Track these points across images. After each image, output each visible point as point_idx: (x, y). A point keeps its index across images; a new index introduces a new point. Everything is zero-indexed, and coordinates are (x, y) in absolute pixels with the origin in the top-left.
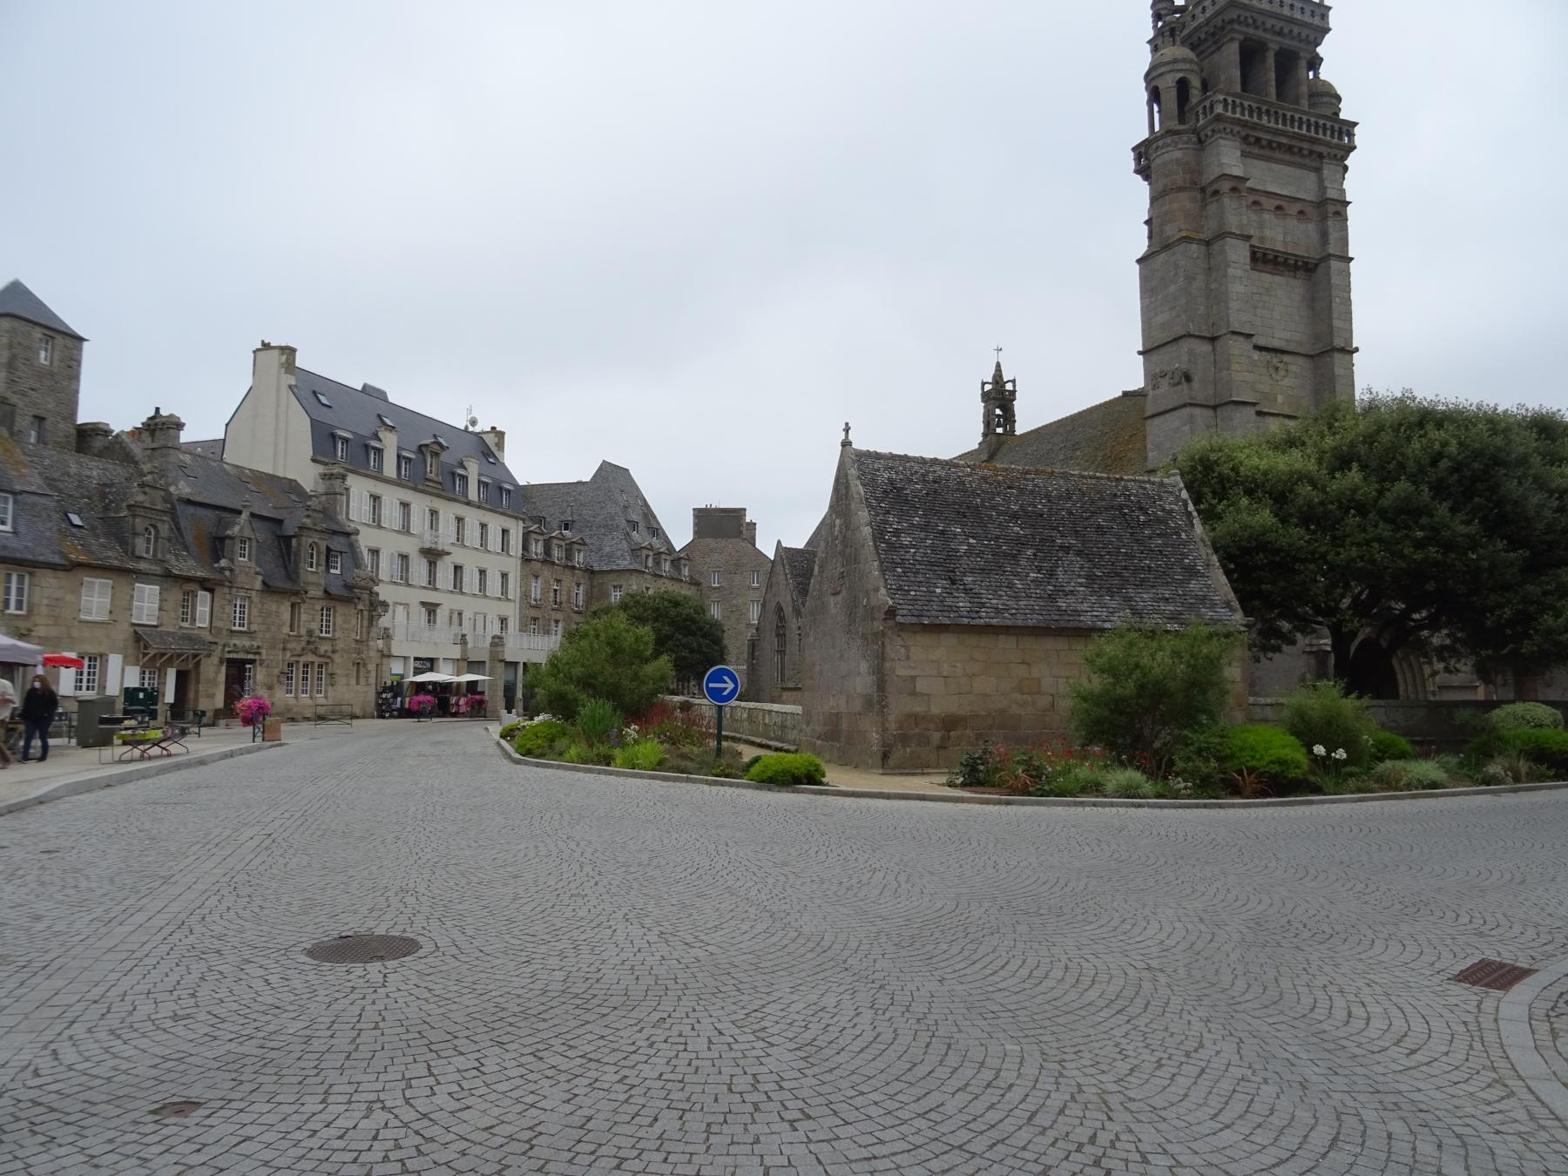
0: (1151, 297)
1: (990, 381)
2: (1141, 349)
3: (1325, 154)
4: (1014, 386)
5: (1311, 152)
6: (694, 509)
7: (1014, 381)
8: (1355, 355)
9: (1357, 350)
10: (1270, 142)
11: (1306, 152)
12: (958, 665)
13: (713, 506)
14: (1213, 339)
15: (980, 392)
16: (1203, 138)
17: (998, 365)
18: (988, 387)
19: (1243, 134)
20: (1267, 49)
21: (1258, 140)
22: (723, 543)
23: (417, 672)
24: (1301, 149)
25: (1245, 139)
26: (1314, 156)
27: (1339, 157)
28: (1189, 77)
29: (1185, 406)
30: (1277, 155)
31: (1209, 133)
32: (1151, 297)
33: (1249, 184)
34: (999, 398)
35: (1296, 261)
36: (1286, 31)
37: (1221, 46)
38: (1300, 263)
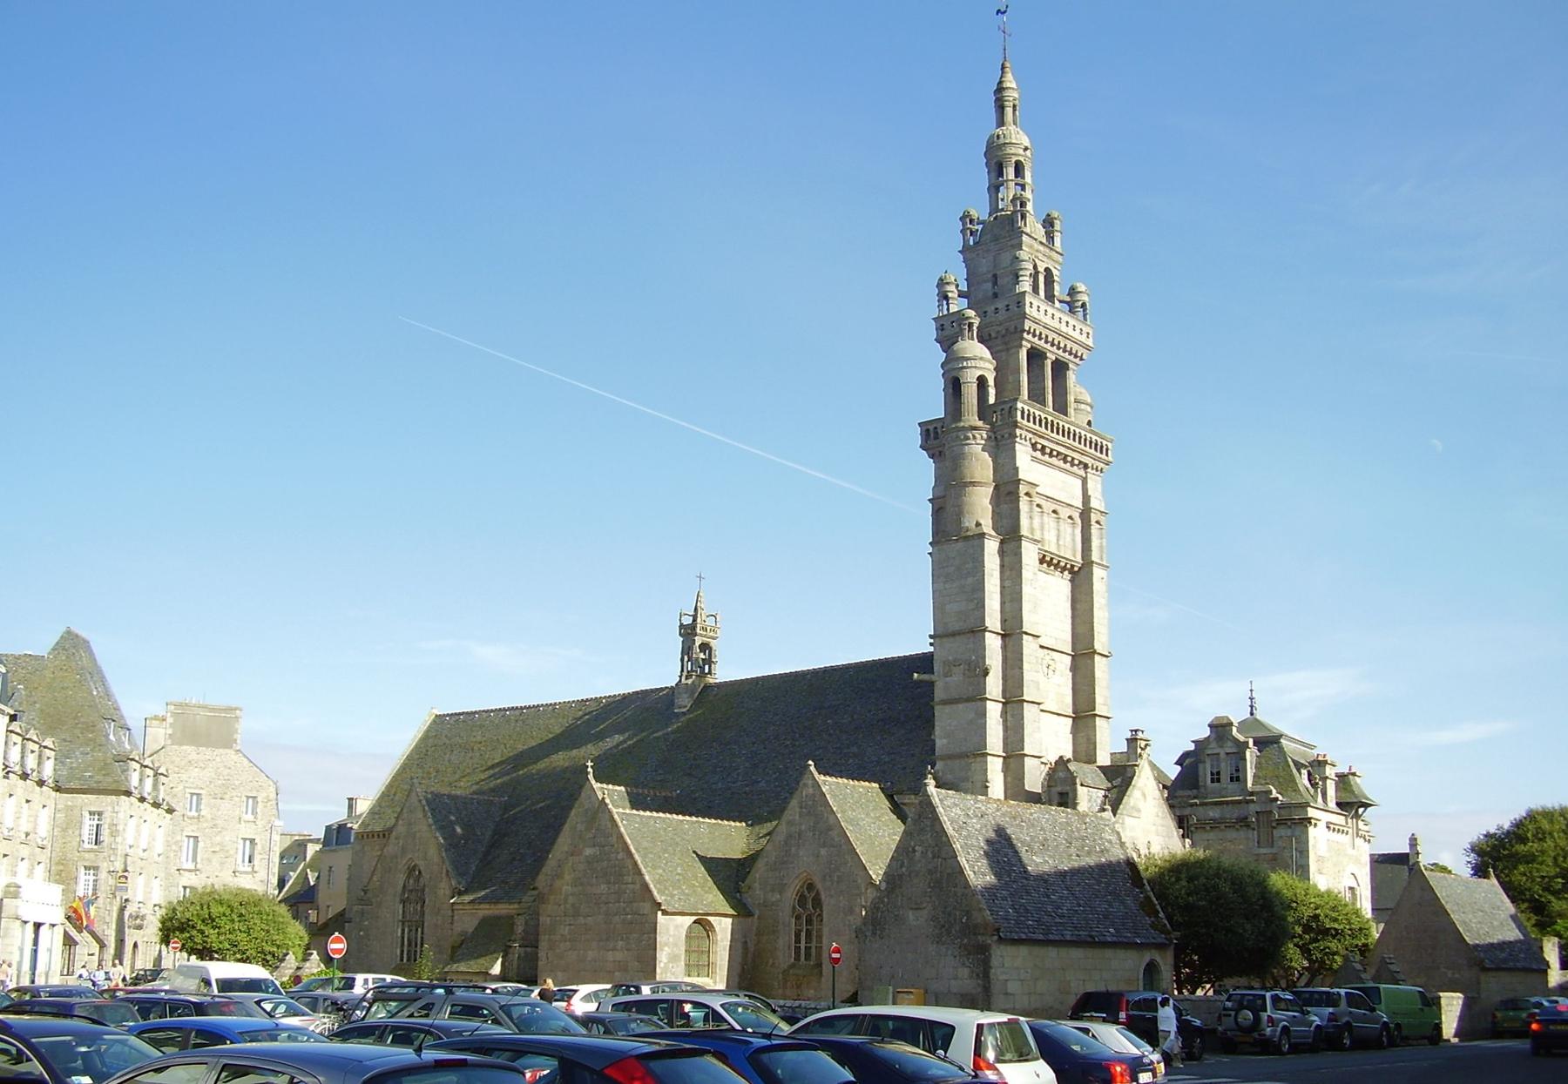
0: (944, 583)
2: (932, 633)
3: (1090, 465)
5: (1080, 462)
10: (1052, 450)
11: (1076, 462)
12: (1029, 971)
16: (999, 437)
19: (1033, 441)
20: (1046, 358)
21: (1044, 447)
22: (207, 753)
23: (1234, 990)
24: (1073, 459)
25: (1034, 446)
26: (1081, 466)
28: (986, 375)
30: (1054, 460)
31: (1006, 436)
32: (944, 583)
33: (1038, 490)
34: (1155, 799)
35: (1066, 564)
37: (1012, 348)
38: (1068, 566)
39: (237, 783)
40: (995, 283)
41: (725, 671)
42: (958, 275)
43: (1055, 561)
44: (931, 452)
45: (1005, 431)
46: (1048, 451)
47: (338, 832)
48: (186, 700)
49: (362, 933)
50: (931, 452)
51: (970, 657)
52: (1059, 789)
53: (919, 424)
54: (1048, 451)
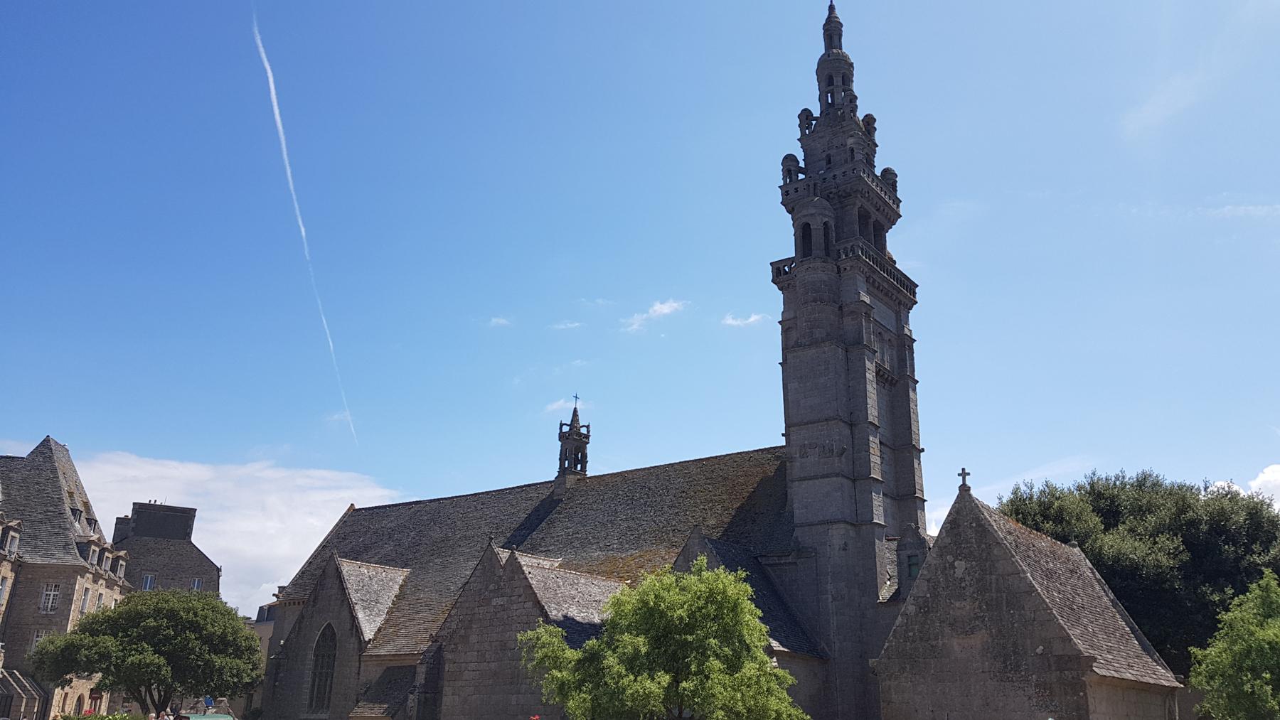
1: (569, 423)
4: (588, 432)
5: (897, 298)
6: (134, 504)
7: (588, 427)
8: (922, 454)
9: (923, 450)
13: (158, 503)
14: (851, 425)
15: (558, 431)
17: (575, 411)
18: (566, 429)
21: (874, 281)
27: (908, 306)
29: (837, 475)
32: (800, 383)
36: (882, 208)
37: (846, 206)
38: (890, 378)
39: (186, 567)
40: (829, 162)
41: (599, 463)
42: (800, 156)
43: (881, 373)
44: (781, 285)
45: (848, 264)
46: (877, 284)
47: (268, 611)
48: (150, 501)
49: (277, 684)
50: (781, 285)
51: (825, 441)
52: (909, 552)
53: (771, 264)
54: (877, 284)
